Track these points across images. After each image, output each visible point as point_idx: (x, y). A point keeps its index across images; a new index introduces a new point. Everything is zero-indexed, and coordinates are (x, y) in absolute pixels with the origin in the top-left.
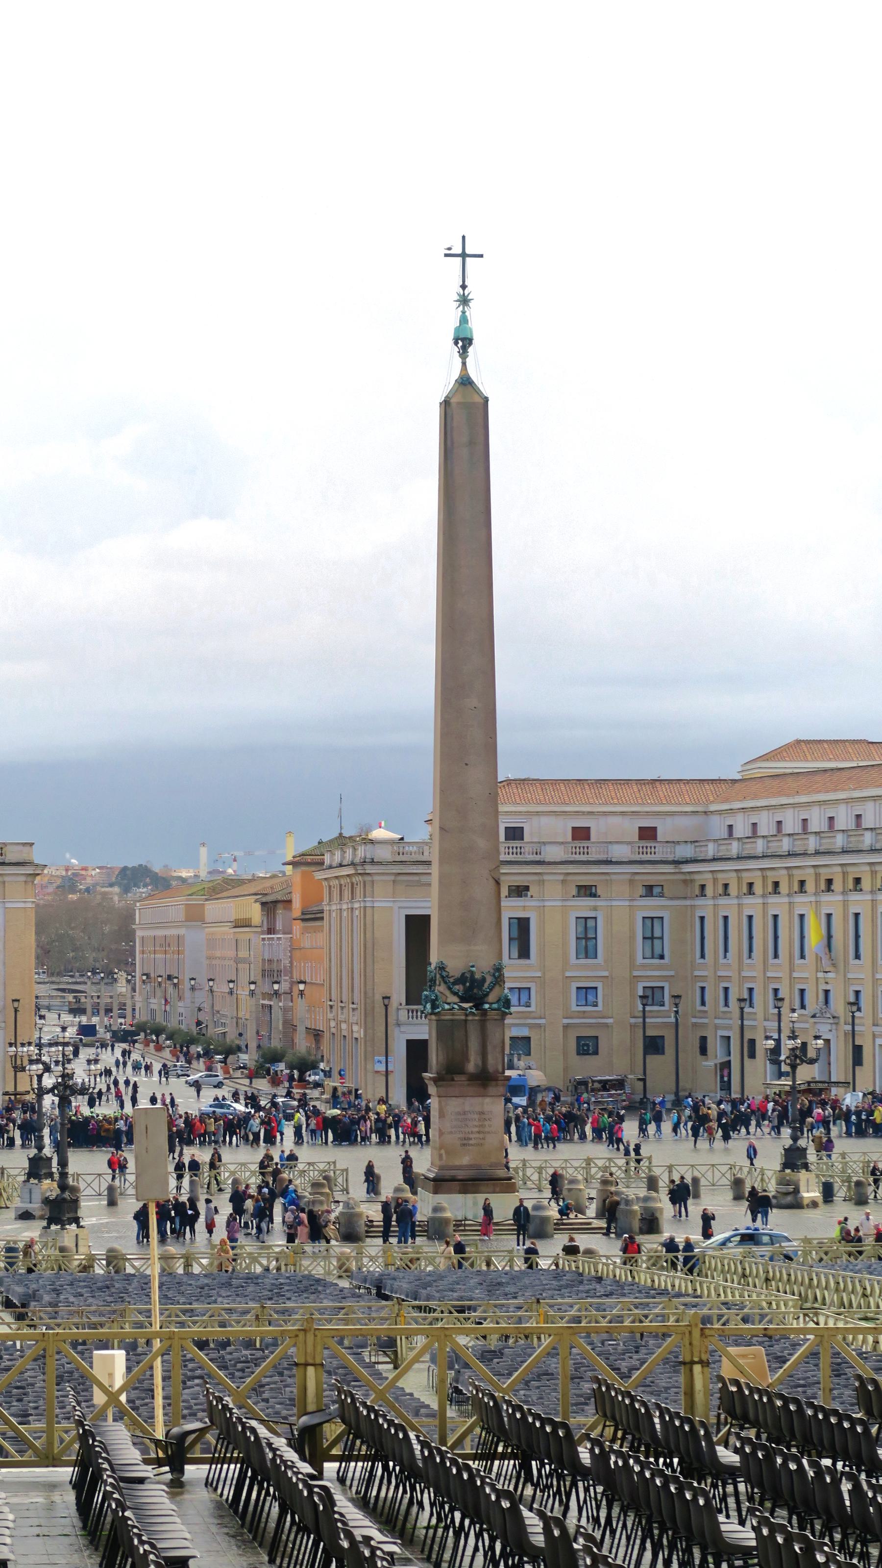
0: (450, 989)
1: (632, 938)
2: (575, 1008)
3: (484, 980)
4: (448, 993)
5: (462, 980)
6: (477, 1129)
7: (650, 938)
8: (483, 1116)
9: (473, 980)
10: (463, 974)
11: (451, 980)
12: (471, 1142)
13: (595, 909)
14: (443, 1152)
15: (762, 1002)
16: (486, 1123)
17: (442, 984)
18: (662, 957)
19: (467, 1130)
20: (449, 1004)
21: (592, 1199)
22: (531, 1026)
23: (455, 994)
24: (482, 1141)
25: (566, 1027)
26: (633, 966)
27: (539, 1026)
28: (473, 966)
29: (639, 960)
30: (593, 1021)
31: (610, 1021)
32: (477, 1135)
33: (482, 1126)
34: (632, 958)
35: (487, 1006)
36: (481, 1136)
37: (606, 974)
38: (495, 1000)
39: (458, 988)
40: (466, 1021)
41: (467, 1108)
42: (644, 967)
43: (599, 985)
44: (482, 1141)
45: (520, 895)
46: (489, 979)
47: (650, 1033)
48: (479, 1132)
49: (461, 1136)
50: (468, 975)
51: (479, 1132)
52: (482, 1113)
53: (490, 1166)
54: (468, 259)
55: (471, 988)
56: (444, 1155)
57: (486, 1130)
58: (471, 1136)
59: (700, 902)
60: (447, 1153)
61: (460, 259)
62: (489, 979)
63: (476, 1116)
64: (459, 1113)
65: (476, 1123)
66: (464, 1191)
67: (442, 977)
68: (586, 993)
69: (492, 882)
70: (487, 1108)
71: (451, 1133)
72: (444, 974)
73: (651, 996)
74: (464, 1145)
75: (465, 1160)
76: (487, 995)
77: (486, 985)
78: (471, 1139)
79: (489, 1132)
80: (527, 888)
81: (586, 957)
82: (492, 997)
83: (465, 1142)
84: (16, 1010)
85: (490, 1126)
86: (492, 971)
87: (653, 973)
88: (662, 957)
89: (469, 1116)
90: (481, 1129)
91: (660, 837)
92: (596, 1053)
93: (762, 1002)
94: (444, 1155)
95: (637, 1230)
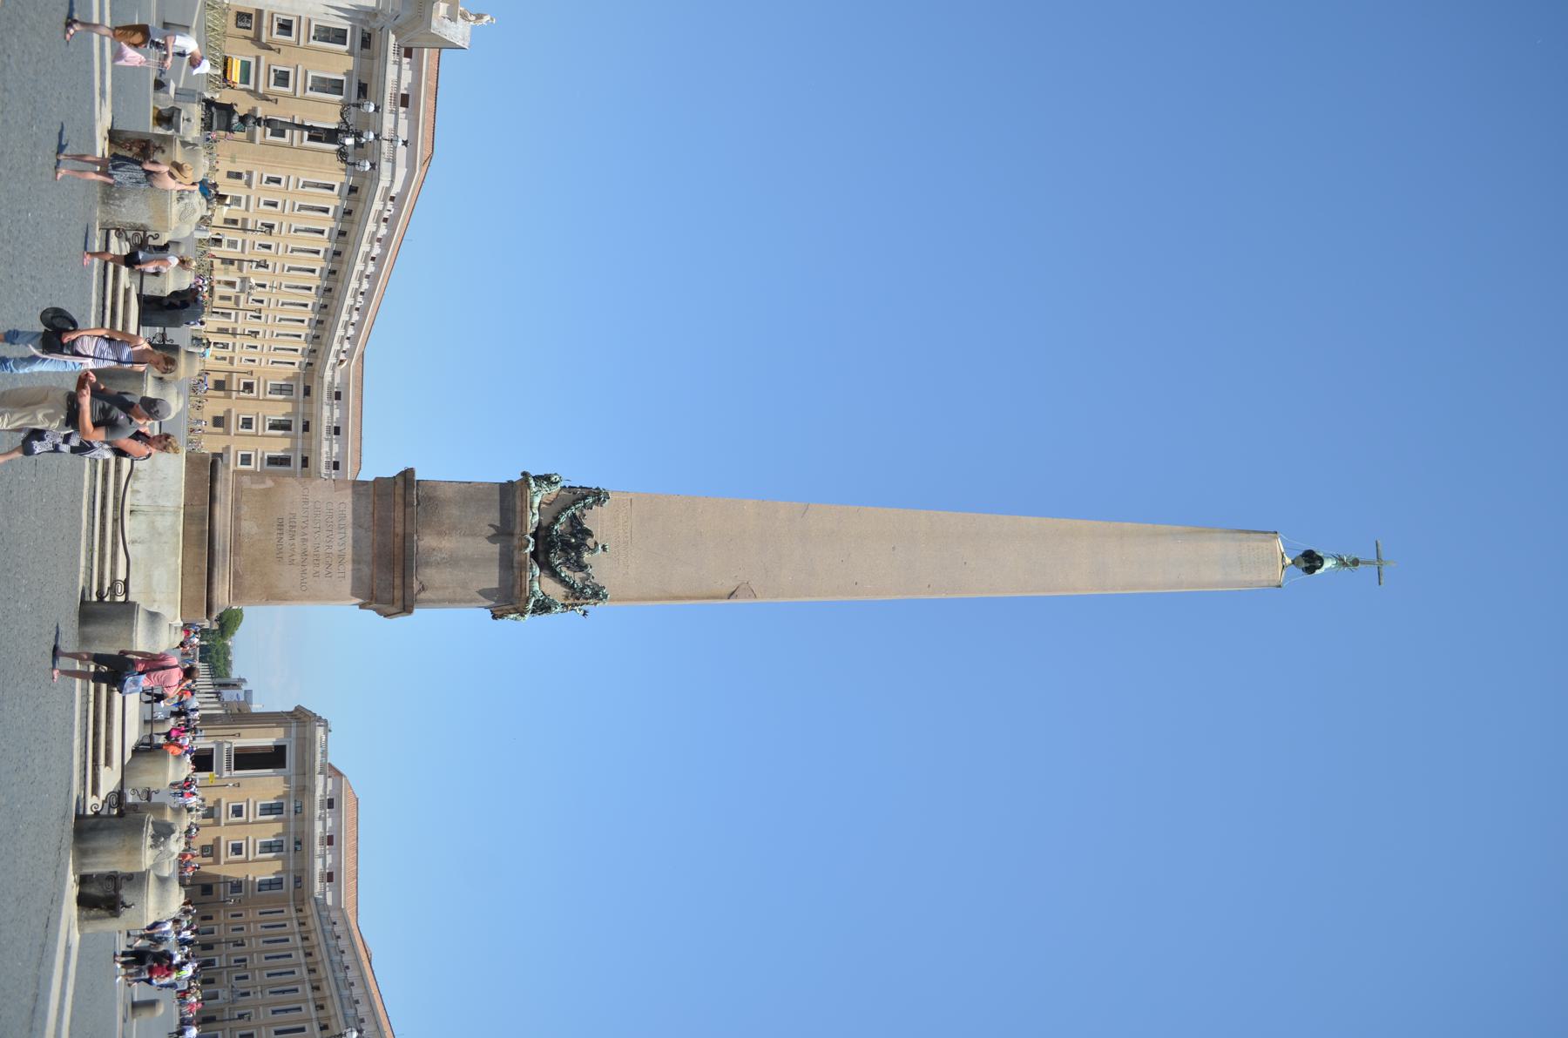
6: (310, 550)
9: (579, 548)
10: (589, 533)
12: (286, 538)
16: (322, 569)
21: (149, 799)
35: (537, 571)
36: (298, 558)
40: (512, 535)
44: (286, 560)
46: (577, 578)
48: (304, 553)
49: (299, 520)
50: (590, 542)
51: (304, 553)
55: (566, 547)
57: (309, 568)
58: (298, 540)
59: (293, 909)
62: (577, 578)
63: (335, 549)
65: (322, 550)
69: (730, 585)
71: (306, 502)
72: (590, 500)
74: (281, 525)
75: (248, 526)
76: (554, 574)
77: (569, 573)
78: (292, 538)
79: (304, 572)
83: (286, 527)
85: (316, 574)
90: (310, 559)
95: (87, 871)
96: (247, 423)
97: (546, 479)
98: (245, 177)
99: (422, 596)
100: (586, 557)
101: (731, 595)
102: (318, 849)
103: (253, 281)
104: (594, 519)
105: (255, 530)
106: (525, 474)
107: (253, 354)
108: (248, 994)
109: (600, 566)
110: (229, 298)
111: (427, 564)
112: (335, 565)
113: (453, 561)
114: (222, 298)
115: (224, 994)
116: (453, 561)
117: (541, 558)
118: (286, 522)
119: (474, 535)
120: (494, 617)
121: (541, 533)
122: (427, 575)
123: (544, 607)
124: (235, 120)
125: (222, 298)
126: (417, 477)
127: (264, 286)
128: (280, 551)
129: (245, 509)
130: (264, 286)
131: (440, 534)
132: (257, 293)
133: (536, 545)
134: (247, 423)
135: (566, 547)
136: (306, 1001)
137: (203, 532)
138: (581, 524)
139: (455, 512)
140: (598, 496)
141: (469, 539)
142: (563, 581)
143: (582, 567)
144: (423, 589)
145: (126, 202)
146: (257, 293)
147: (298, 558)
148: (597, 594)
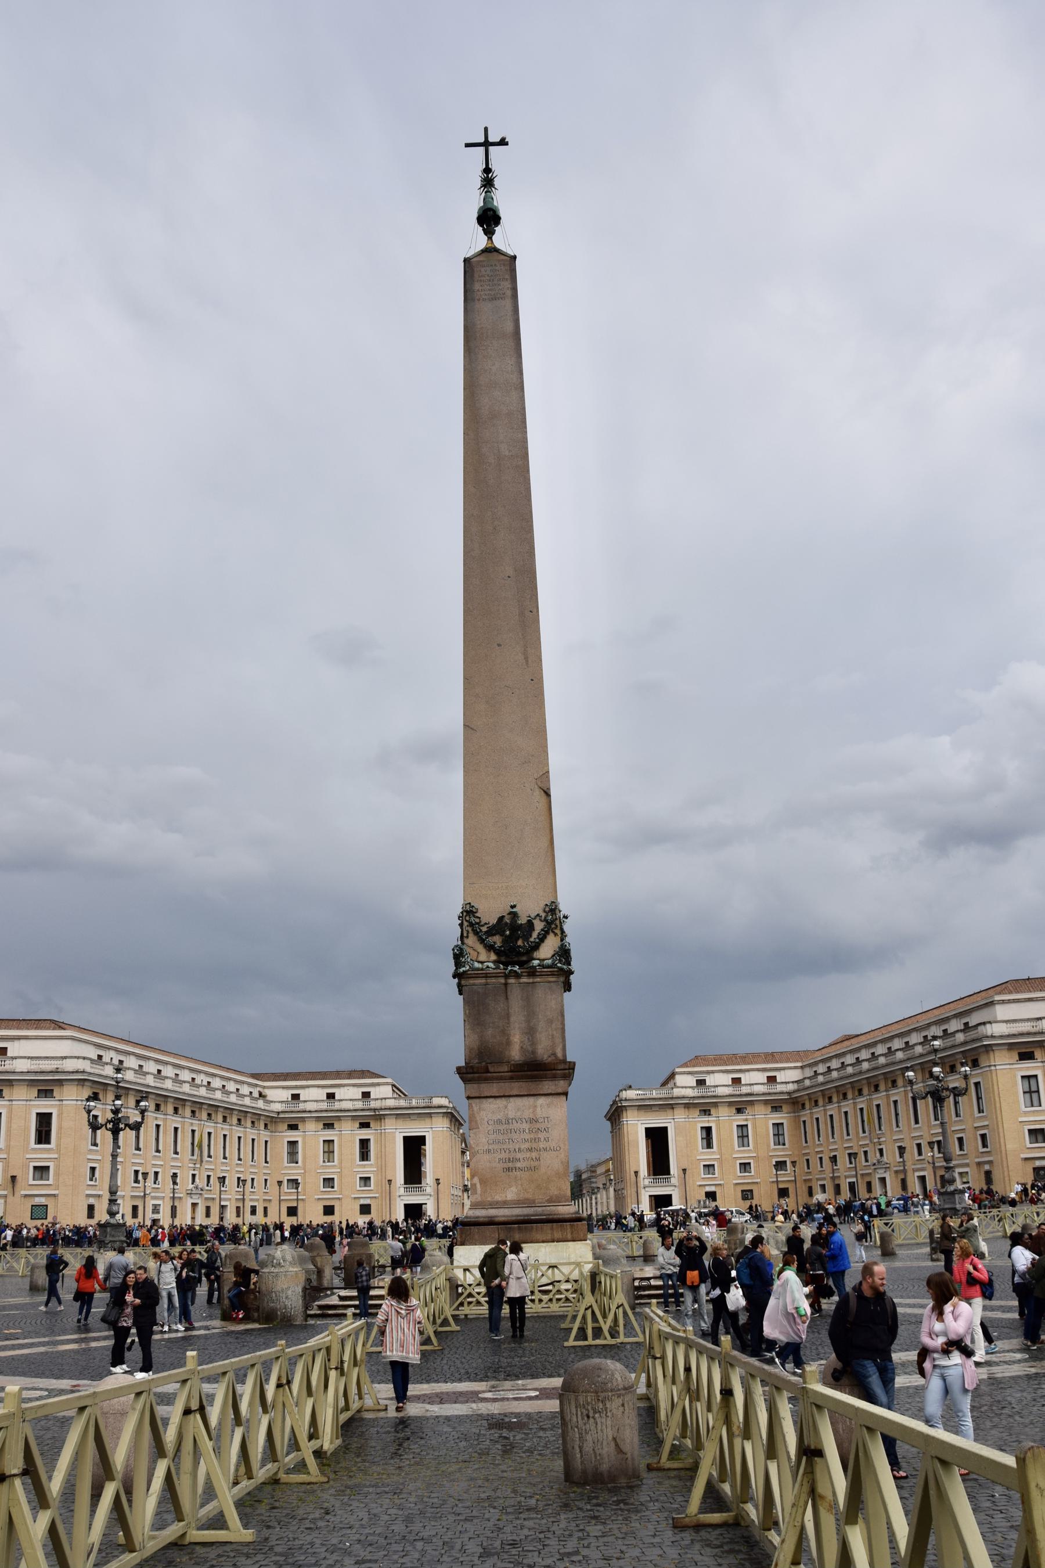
0: (482, 941)
1: (768, 1135)
3: (530, 924)
4: (480, 948)
7: (777, 1135)
8: (538, 1125)
9: (515, 927)
10: (501, 918)
11: (484, 929)
12: (518, 1165)
13: (746, 1120)
14: (476, 1180)
15: (843, 1161)
16: (542, 1136)
17: (471, 935)
18: (784, 1144)
19: (511, 1146)
20: (482, 963)
23: (490, 948)
24: (536, 1163)
26: (769, 1150)
28: (513, 907)
29: (772, 1146)
32: (528, 1155)
33: (537, 1140)
34: (769, 1146)
35: (536, 962)
36: (534, 1155)
38: (550, 956)
39: (497, 940)
41: (511, 1114)
42: (775, 1150)
43: (751, 1161)
44: (536, 1163)
46: (539, 926)
47: (781, 1186)
48: (530, 1150)
49: (503, 1155)
50: (507, 920)
51: (530, 1150)
52: (533, 1121)
53: (550, 1201)
54: (491, 148)
56: (478, 1186)
58: (519, 1155)
60: (483, 1182)
61: (482, 149)
62: (539, 926)
63: (526, 1126)
64: (499, 1122)
65: (527, 1136)
67: (471, 925)
68: (745, 1167)
69: (538, 793)
70: (540, 1113)
71: (489, 1151)
73: (780, 1165)
74: (508, 1169)
75: (511, 1194)
76: (536, 947)
77: (535, 935)
79: (545, 1149)
83: (510, 1165)
85: (547, 1140)
86: (543, 915)
87: (781, 1153)
88: (784, 1144)
89: (515, 1126)
90: (534, 1145)
91: (778, 1080)
93: (843, 1161)
94: (478, 1186)
96: (329, 1182)
97: (458, 956)
98: (92, 1201)
99: (560, 1055)
100: (523, 920)
101: (547, 794)
102: (745, 1090)
103: (191, 1186)
104: (490, 913)
105: (514, 1189)
106: (454, 977)
107: (259, 1183)
108: (881, 1151)
109: (530, 908)
110: (208, 1208)
111: (534, 1052)
112: (538, 1125)
113: (530, 1032)
114: (208, 1215)
115: (880, 1174)
116: (530, 1032)
117: (524, 958)
118: (506, 1166)
119: (508, 1016)
120: (569, 990)
121: (503, 959)
122: (542, 1052)
123: (564, 953)
124: (112, 1221)
125: (208, 1215)
126: (463, 1064)
127: (194, 1176)
128: (530, 1169)
129: (498, 1198)
130: (194, 1176)
131: (508, 1043)
132: (201, 1182)
133: (513, 964)
134: (329, 1182)
135: (513, 937)
136: (888, 1096)
137: (519, 1228)
138: (494, 926)
139: (490, 1032)
140: (468, 913)
141: (512, 1019)
142: (542, 939)
143: (530, 924)
144: (554, 1054)
145: (288, 1303)
146: (201, 1182)
147: (534, 1155)
148: (552, 909)
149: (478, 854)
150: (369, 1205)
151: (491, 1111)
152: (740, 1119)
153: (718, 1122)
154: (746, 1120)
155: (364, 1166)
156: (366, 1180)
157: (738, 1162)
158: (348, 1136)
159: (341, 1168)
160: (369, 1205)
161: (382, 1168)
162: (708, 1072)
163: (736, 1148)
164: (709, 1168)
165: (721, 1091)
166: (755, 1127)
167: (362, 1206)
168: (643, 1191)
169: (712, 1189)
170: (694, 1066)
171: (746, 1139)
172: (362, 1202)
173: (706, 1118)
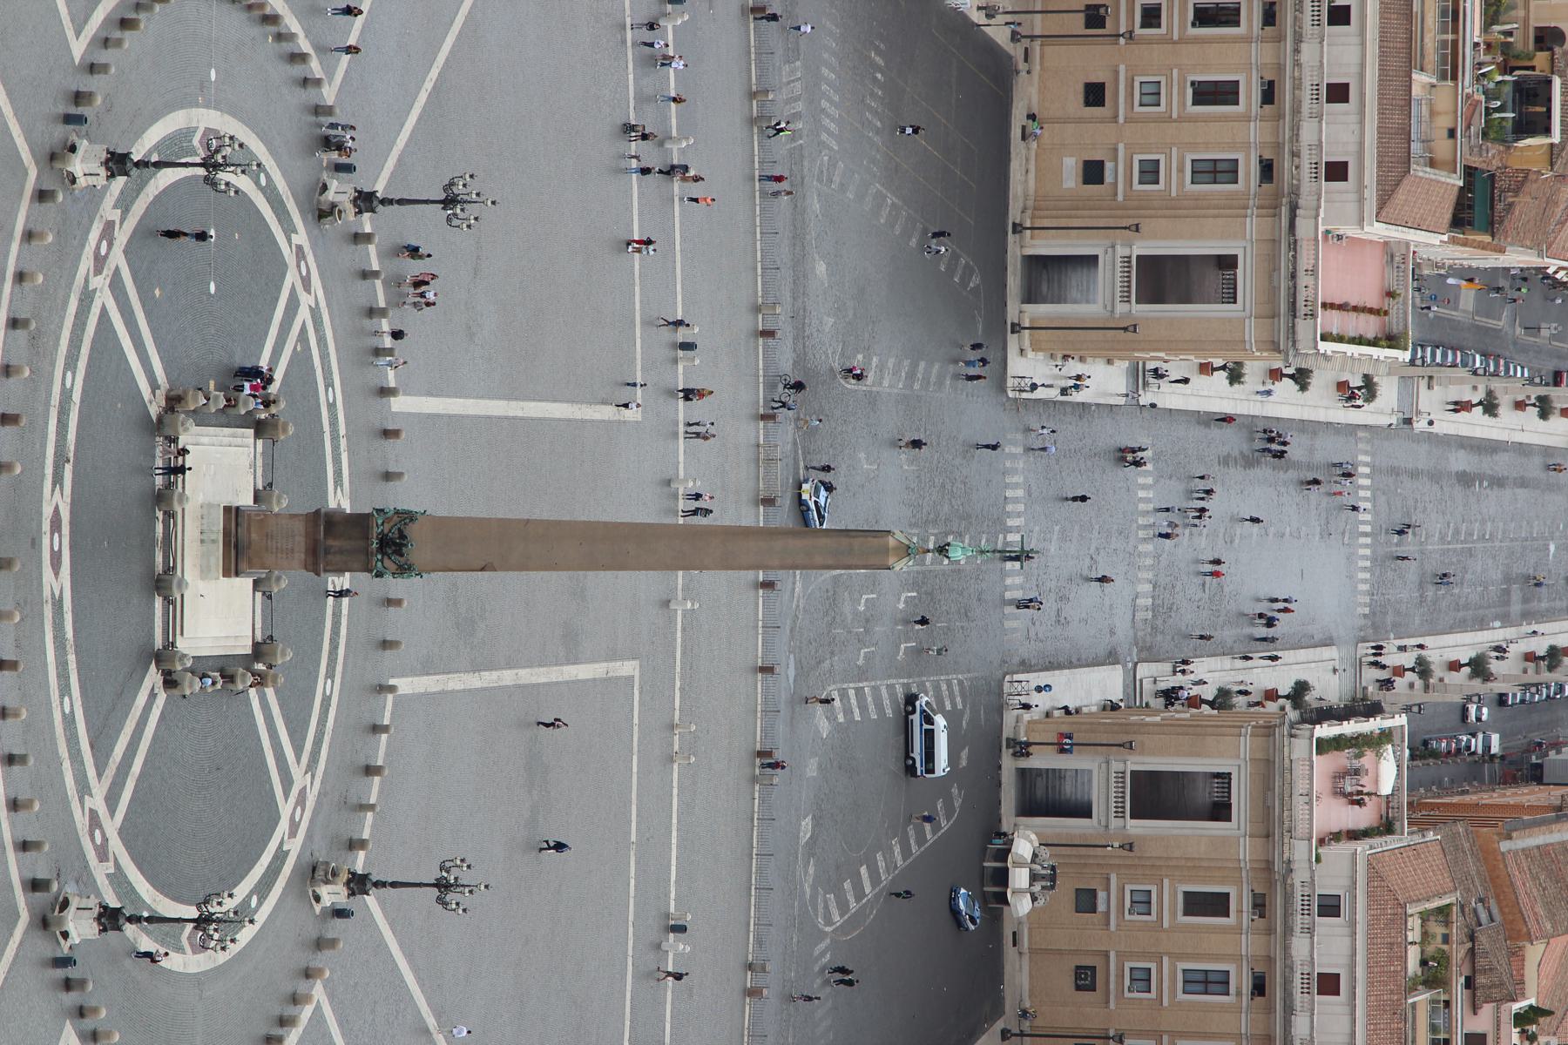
2: (1128, 965)
5: (402, 536)
13: (1239, 994)
22: (1108, 913)
25: (1106, 955)
27: (1108, 924)
30: (1112, 986)
31: (1112, 1005)
37: (1165, 1003)
39: (395, 534)
45: (1255, 906)
55: (395, 544)
62: (402, 560)
66: (226, 533)
68: (1143, 979)
75: (254, 536)
80: (1262, 916)
81: (1185, 982)
82: (387, 562)
84: (1125, 329)
92: (1078, 988)
101: (482, 569)
113: (341, 552)
116: (341, 552)
134: (1153, 95)
149: (447, 527)
150: (1101, 181)
151: (299, 527)
152: (1241, 980)
153: (1237, 930)
154: (1239, 994)
155: (1181, 170)
156: (1150, 172)
157: (1153, 966)
158: (1240, 133)
159: (1180, 120)
160: (1101, 181)
161: (1174, 208)
162: (1353, 924)
163: (1182, 966)
164: (1143, 903)
165: (1300, 946)
166: (1223, 1008)
167: (1100, 165)
168: (1100, 759)
169: (1101, 907)
170: (1370, 895)
171: (1200, 987)
172: (1109, 166)
173: (1247, 904)
